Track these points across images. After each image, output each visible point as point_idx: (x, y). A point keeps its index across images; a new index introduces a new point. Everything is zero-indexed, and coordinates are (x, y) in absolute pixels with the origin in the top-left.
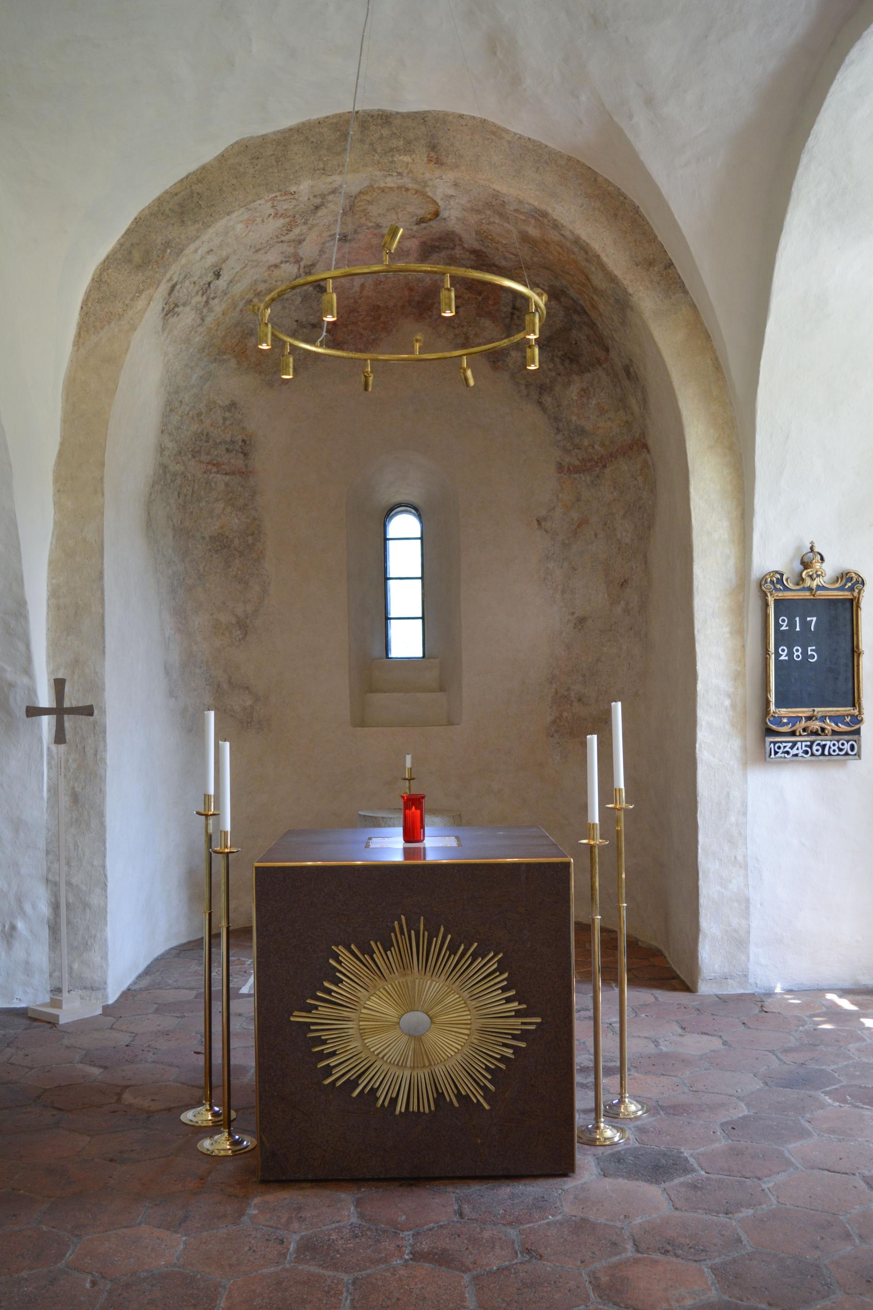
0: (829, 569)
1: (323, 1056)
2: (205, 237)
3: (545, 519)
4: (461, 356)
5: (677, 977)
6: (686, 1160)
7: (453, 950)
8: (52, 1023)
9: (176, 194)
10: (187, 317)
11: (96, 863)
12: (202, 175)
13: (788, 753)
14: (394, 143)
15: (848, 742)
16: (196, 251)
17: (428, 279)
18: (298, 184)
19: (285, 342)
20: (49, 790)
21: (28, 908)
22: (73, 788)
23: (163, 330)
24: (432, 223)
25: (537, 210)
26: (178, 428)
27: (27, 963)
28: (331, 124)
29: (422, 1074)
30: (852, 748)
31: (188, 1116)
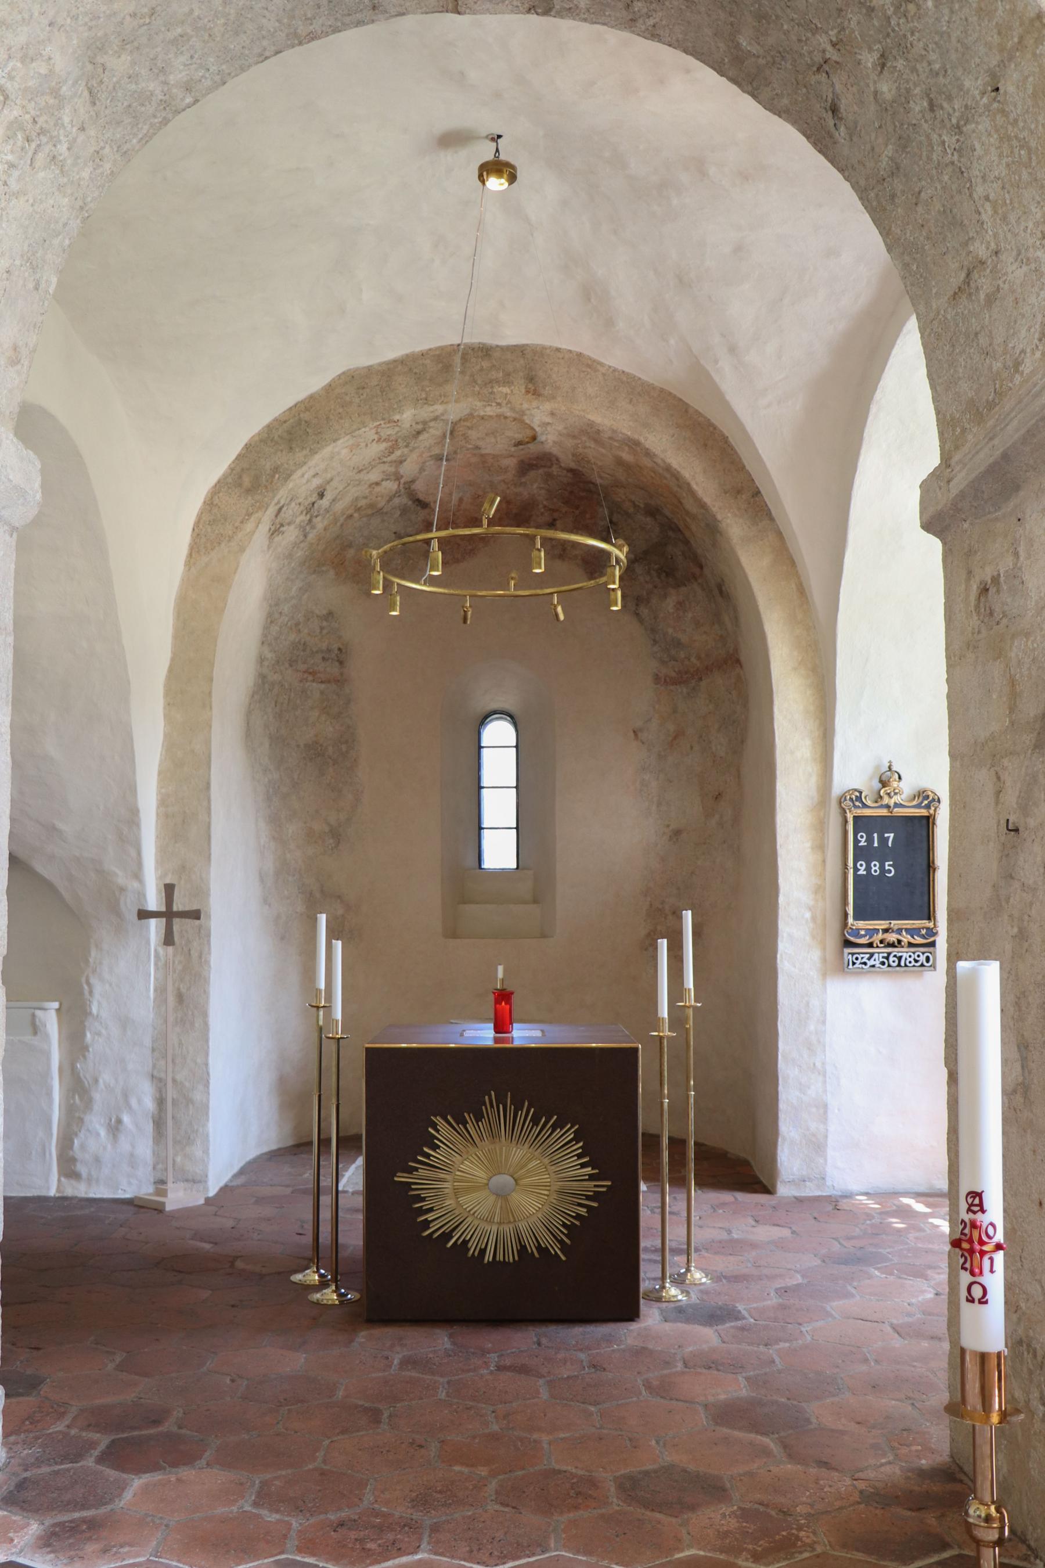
0: (906, 788)
1: (422, 1211)
2: (312, 463)
3: (641, 730)
4: (552, 593)
5: (760, 1182)
6: (739, 1312)
7: (535, 1121)
8: (158, 1209)
9: (285, 422)
10: (291, 534)
11: (199, 1060)
13: (865, 963)
14: (494, 375)
15: (923, 953)
16: (303, 476)
17: (525, 493)
18: (401, 413)
19: (392, 583)
20: (155, 990)
21: (133, 1102)
22: (179, 989)
23: (269, 548)
24: (529, 445)
25: (630, 439)
26: (276, 639)
27: (132, 1155)
28: (434, 356)
29: (508, 1228)
30: (928, 959)
31: (297, 1277)
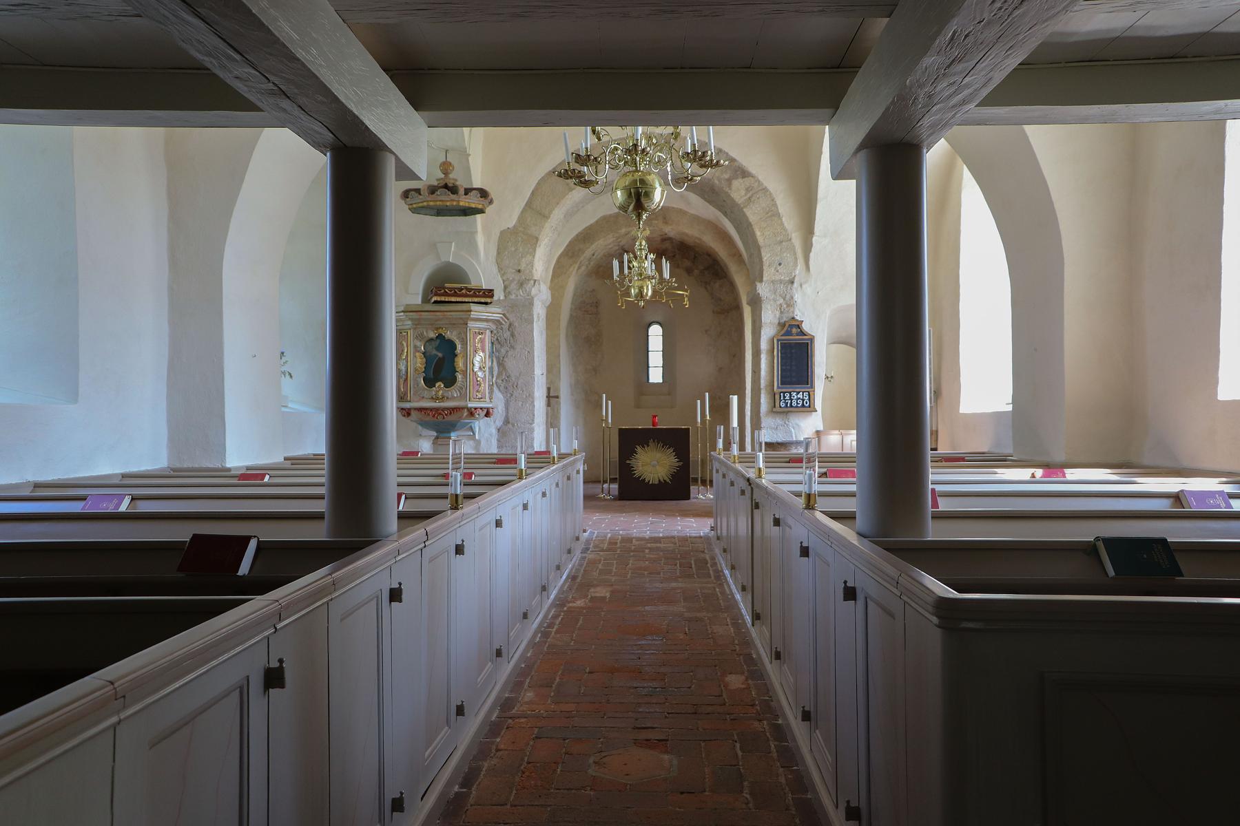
10: (583, 268)
12: (590, 228)
